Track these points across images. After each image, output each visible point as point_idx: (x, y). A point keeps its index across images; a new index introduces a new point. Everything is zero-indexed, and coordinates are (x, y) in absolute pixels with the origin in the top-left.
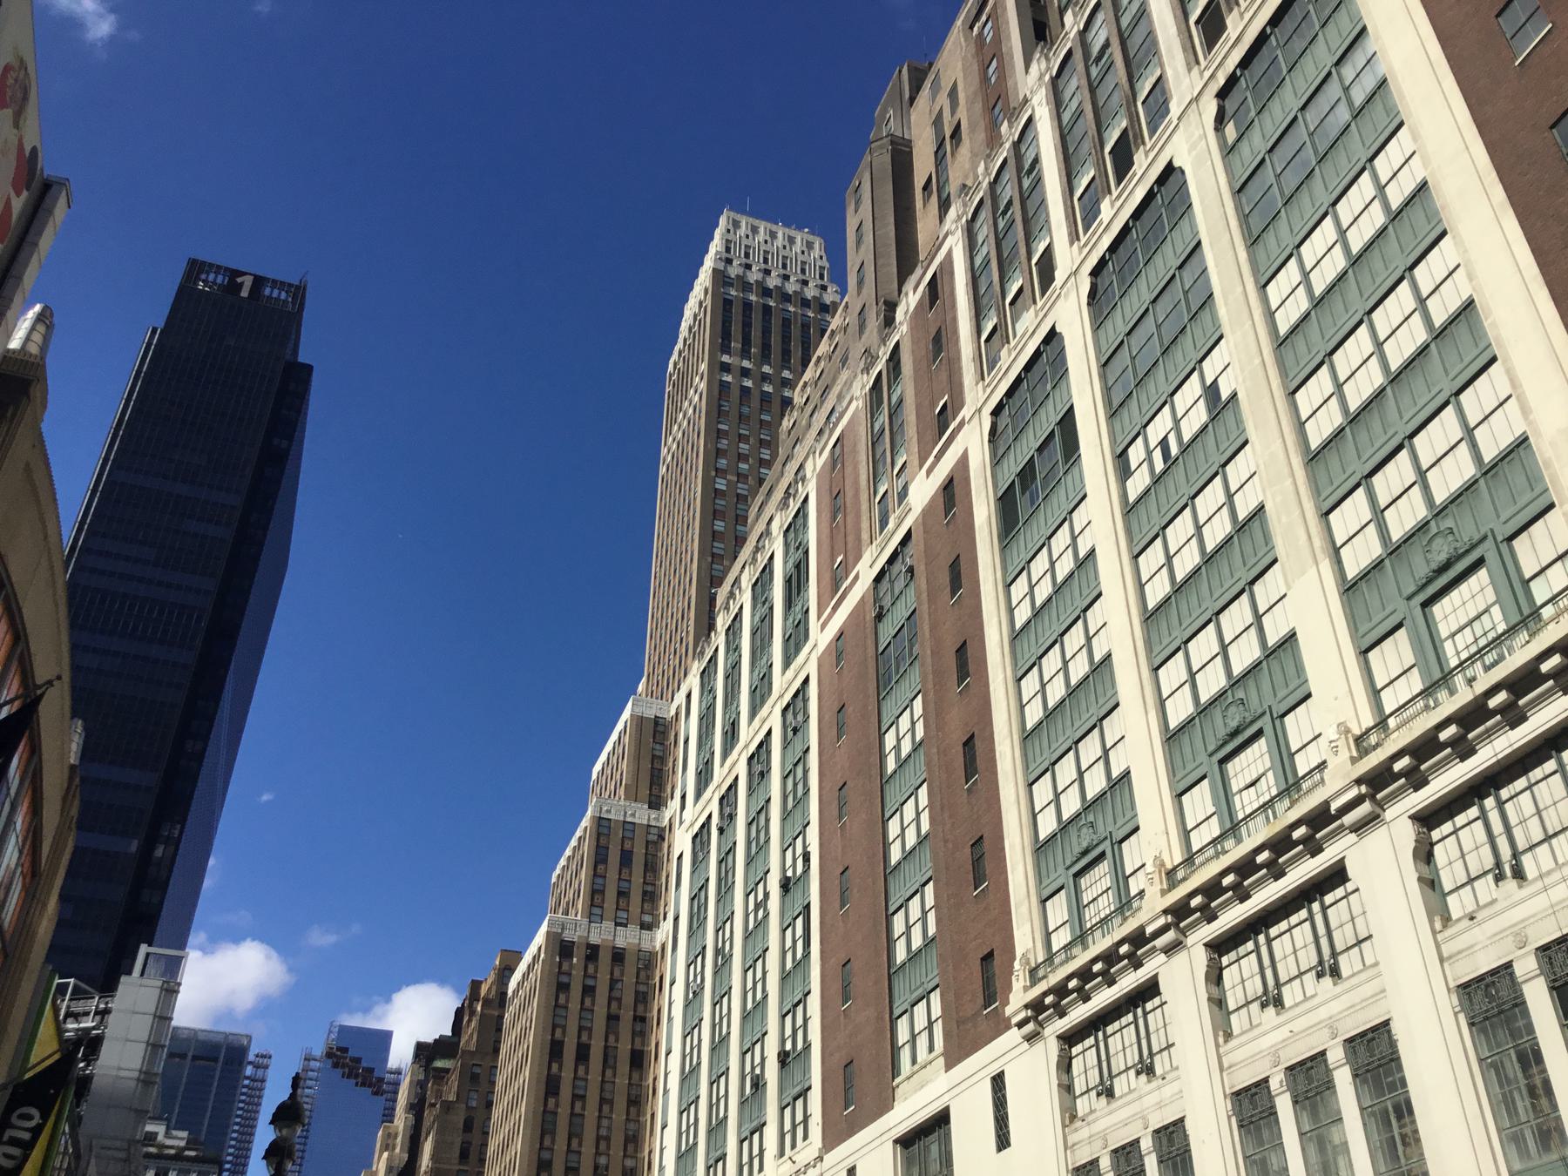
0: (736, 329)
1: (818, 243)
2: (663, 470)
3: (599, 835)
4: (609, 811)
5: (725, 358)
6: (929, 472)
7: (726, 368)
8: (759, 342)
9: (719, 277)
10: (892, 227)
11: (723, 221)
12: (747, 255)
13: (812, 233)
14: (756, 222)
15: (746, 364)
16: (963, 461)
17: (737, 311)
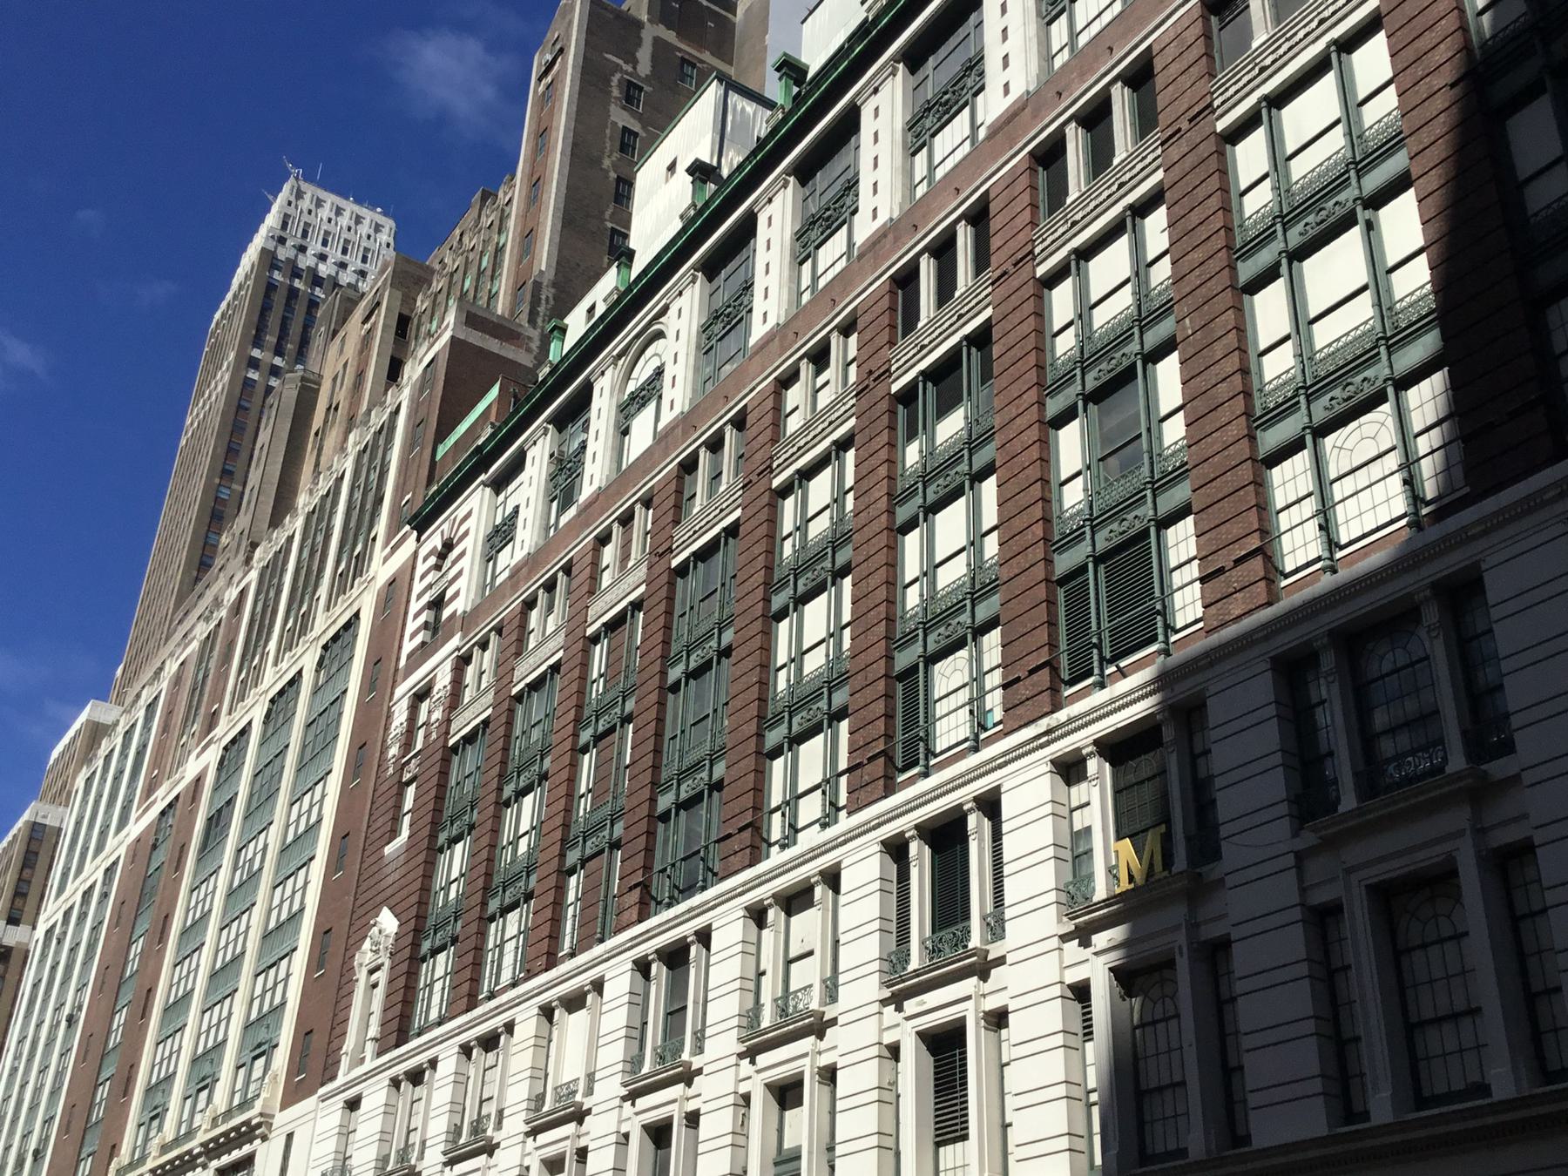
0: (274, 321)
1: (389, 224)
2: (183, 442)
3: (31, 838)
4: (45, 817)
5: (256, 353)
6: (198, 756)
7: (254, 364)
8: (297, 339)
9: (268, 259)
10: (279, 467)
11: (286, 187)
12: (305, 234)
13: (385, 214)
14: (322, 194)
15: (278, 361)
16: (206, 769)
17: (279, 299)
